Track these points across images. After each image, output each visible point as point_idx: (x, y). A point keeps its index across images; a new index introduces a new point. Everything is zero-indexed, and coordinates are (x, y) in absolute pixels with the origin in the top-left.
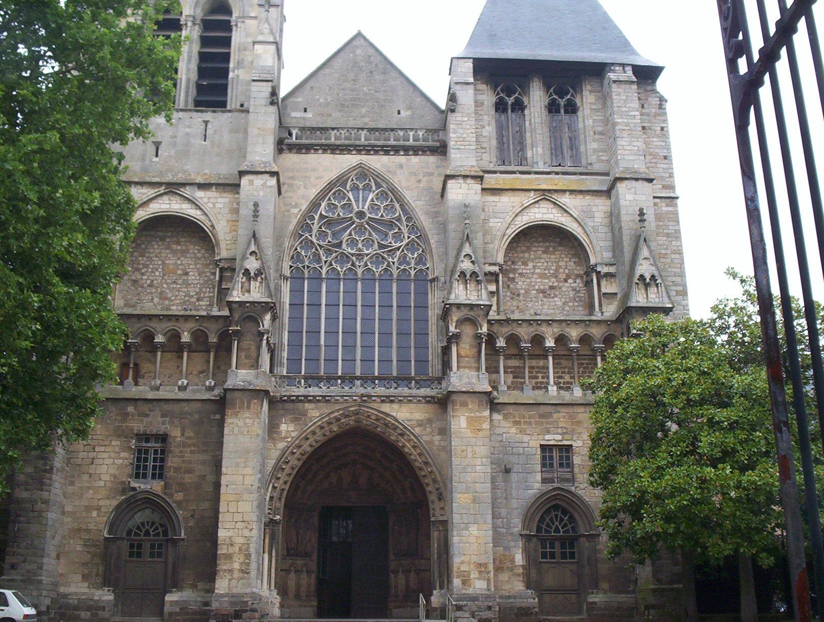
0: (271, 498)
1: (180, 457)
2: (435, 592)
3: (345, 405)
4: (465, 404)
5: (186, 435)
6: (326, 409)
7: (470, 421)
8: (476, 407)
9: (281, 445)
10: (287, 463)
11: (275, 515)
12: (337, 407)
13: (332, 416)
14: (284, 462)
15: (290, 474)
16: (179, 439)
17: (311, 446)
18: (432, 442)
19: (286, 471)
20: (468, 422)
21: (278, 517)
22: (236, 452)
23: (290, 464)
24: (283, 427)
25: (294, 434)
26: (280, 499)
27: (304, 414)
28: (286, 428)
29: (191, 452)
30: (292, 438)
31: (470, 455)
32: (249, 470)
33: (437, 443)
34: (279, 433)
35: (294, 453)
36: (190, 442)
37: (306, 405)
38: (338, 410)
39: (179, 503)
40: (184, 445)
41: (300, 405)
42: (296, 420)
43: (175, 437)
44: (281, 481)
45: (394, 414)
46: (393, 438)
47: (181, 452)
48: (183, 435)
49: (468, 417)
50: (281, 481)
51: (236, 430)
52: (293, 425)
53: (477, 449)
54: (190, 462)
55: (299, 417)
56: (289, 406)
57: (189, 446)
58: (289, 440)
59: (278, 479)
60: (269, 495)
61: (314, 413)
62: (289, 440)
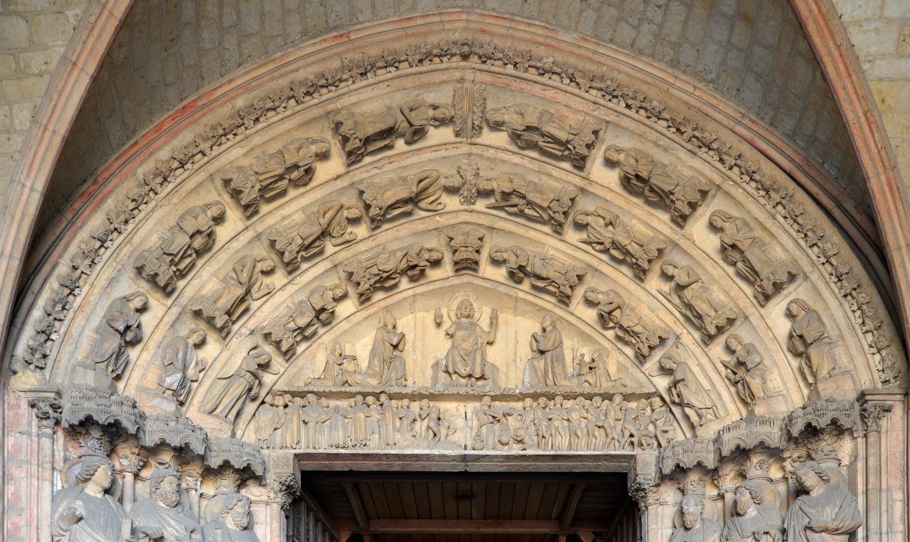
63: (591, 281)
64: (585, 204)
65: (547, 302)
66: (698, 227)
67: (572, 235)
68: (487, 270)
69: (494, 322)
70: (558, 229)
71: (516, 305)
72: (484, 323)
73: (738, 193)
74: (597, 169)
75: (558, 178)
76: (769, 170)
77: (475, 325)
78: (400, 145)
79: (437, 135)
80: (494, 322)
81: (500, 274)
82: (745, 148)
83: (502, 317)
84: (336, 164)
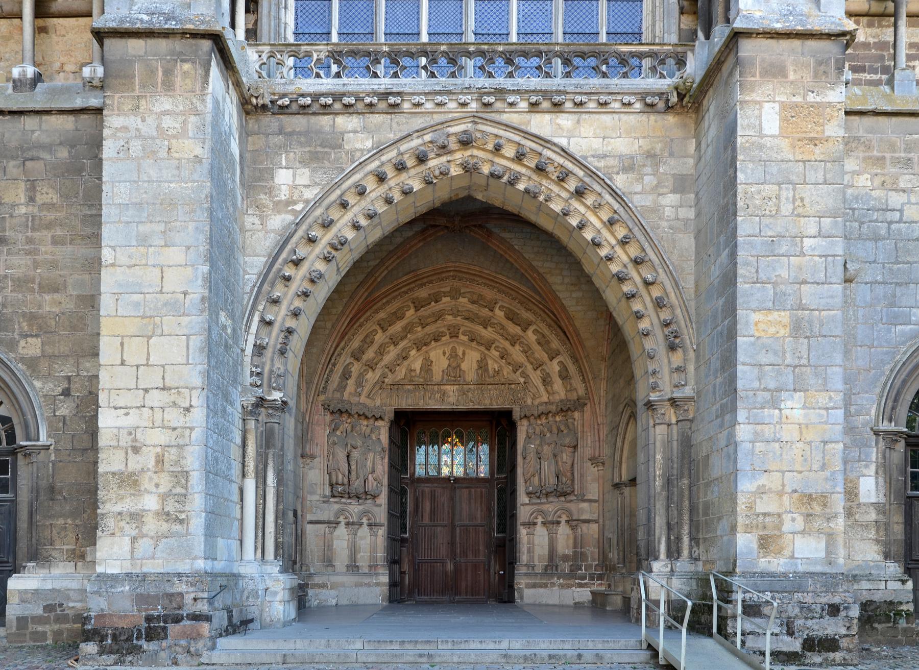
0: (259, 349)
1: (29, 253)
2: (656, 566)
3: (438, 118)
4: (776, 71)
5: (40, 199)
6: (386, 127)
7: (790, 113)
8: (808, 77)
9: (278, 221)
10: (297, 263)
11: (271, 388)
12: (419, 122)
13: (404, 147)
14: (286, 262)
15: (306, 294)
16: (23, 210)
17: (356, 227)
18: (656, 209)
19: (294, 286)
20: (784, 120)
21: (277, 395)
22: (139, 206)
23: (304, 269)
24: (283, 177)
25: (310, 194)
26: (282, 352)
27: (335, 142)
28: (293, 180)
29: (55, 242)
30: (307, 202)
31: (786, 209)
32: (175, 255)
33: (668, 212)
34: (270, 191)
35: (312, 241)
36: (51, 216)
37: (340, 120)
38: (421, 131)
39: (32, 363)
40: (35, 224)
41: (325, 121)
42: (313, 159)
43: (14, 206)
44: (283, 309)
45: (563, 142)
46: (556, 206)
47: (30, 241)
48: (32, 199)
49: (784, 106)
50: (283, 309)
51: (136, 147)
52: (307, 171)
53: (807, 192)
54: (54, 265)
55: (322, 150)
56: (298, 122)
57: (49, 226)
58: (299, 207)
59: (276, 302)
60: (251, 340)
61: (358, 135)
62: (299, 207)
63: (497, 344)
64: (493, 321)
65: (482, 348)
66: (530, 332)
67: (489, 329)
68: (462, 337)
69: (464, 354)
70: (485, 328)
71: (472, 348)
72: (460, 354)
73: (541, 325)
74: (497, 311)
75: (485, 312)
76: (549, 320)
77: (457, 355)
78: (433, 303)
79: (445, 300)
80: (464, 354)
81: (466, 338)
82: (542, 313)
83: (467, 351)
84: (412, 311)
